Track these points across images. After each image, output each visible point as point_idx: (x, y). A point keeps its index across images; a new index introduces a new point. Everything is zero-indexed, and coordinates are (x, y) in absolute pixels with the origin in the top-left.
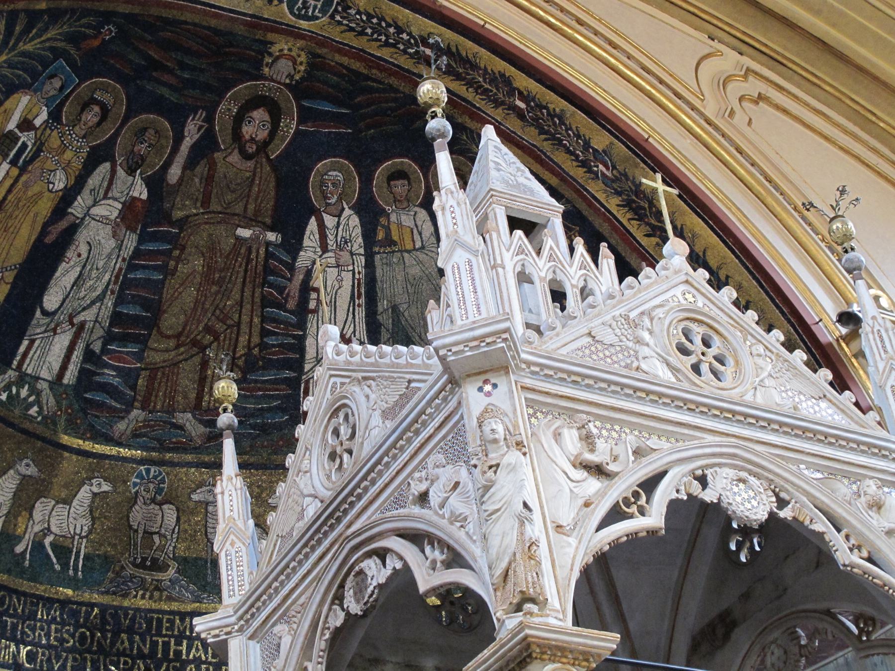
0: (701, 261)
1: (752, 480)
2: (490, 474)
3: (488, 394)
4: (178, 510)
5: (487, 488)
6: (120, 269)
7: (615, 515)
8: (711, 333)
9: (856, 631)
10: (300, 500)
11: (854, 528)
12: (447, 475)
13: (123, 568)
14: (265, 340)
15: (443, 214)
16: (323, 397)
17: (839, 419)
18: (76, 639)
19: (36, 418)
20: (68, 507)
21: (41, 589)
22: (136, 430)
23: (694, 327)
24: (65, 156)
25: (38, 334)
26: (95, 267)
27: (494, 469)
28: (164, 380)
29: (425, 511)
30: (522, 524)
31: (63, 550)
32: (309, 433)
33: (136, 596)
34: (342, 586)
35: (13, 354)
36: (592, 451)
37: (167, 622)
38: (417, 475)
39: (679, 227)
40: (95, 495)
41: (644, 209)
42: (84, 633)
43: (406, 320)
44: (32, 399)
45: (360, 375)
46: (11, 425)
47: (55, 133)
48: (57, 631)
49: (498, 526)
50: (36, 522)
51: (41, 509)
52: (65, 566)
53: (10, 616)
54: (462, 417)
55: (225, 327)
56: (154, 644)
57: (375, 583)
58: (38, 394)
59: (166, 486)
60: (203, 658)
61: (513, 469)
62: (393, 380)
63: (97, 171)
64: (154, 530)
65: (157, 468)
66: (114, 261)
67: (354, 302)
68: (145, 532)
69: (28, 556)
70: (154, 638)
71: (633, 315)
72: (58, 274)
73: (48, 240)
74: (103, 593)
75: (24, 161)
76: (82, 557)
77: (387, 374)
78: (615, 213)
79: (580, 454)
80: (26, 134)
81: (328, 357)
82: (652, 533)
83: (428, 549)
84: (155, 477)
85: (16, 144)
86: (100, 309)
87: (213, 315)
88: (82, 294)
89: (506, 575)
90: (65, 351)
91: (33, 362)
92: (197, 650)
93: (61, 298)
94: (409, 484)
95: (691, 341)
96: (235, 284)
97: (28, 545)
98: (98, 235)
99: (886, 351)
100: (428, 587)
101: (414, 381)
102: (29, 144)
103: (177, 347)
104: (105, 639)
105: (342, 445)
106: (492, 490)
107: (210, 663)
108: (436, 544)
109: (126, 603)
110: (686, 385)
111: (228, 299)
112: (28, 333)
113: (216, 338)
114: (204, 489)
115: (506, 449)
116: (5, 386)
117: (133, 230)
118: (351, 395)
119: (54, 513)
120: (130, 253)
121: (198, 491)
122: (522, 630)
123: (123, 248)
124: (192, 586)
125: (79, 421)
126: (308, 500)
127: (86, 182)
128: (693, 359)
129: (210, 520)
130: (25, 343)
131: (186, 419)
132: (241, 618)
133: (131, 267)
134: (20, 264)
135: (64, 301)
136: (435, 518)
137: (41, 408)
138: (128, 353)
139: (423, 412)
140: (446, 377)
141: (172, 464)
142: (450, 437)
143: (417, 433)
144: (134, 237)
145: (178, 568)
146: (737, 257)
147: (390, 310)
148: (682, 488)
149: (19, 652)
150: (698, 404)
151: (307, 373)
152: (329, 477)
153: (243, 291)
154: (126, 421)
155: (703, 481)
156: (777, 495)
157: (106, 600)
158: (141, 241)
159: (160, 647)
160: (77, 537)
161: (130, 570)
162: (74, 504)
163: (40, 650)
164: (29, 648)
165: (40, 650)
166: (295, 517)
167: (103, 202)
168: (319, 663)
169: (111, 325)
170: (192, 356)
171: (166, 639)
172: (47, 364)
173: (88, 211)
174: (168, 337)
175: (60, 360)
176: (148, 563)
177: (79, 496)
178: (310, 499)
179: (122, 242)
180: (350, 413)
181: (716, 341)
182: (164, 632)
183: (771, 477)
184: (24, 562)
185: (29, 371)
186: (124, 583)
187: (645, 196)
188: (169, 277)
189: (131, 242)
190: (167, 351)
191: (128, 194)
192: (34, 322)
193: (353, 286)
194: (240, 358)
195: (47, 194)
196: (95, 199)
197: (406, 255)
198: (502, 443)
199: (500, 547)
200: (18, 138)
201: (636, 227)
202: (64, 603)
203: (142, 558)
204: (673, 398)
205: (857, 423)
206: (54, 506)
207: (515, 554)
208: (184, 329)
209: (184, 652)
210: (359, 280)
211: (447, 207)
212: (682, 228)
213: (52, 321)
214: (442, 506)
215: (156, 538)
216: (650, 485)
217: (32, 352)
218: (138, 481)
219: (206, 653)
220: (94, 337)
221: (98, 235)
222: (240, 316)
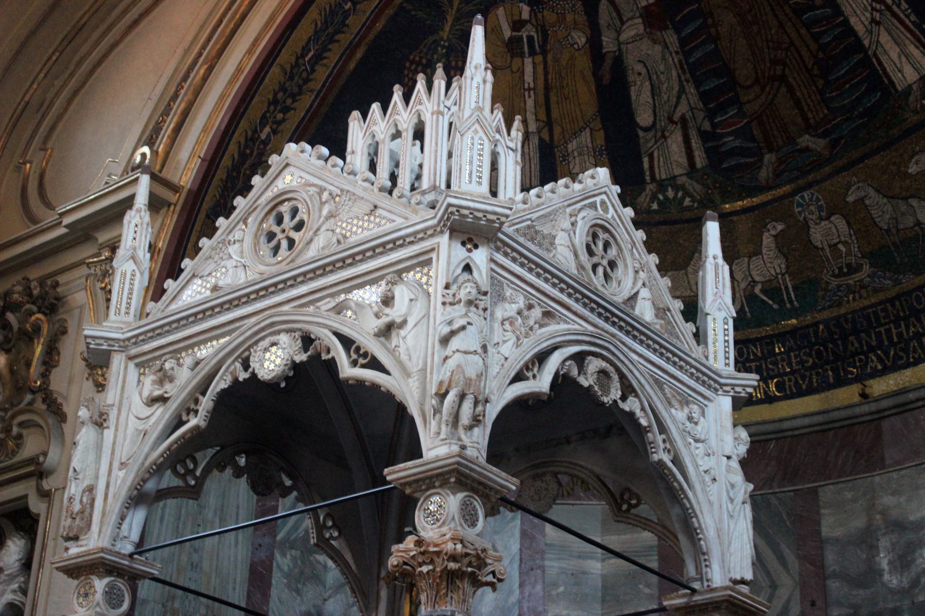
4: (842, 215)
6: (680, 61)
13: (827, 283)
14: (821, 41)
18: (814, 356)
19: (693, 206)
20: (761, 257)
21: (768, 330)
22: (775, 171)
24: (568, 20)
25: (652, 147)
26: (659, 73)
28: (771, 120)
31: (772, 290)
33: (848, 302)
35: (642, 172)
37: (882, 312)
40: (775, 236)
42: (819, 349)
44: (680, 194)
46: (675, 222)
47: (546, 13)
48: (796, 357)
50: (740, 281)
51: (738, 269)
52: (781, 302)
53: (753, 361)
56: (878, 335)
58: (683, 187)
63: (600, 11)
64: (835, 241)
65: (808, 192)
66: (670, 59)
68: (830, 246)
69: (747, 309)
70: (877, 330)
72: (634, 98)
73: (606, 80)
74: (820, 311)
75: (539, 47)
76: (791, 290)
80: (524, 30)
84: (811, 200)
85: (523, 41)
86: (688, 99)
87: (769, 48)
88: (665, 97)
90: (683, 145)
91: (662, 170)
92: (915, 326)
93: (651, 111)
96: (766, 14)
97: (742, 302)
98: (641, 50)
102: (532, 34)
103: (763, 89)
104: (837, 346)
109: (843, 311)
111: (770, 29)
112: (643, 151)
114: (853, 188)
116: (650, 199)
117: (666, 28)
119: (751, 267)
120: (678, 45)
121: (850, 193)
123: (669, 45)
124: (888, 275)
125: (729, 189)
127: (598, 24)
129: (873, 212)
130: (646, 160)
131: (806, 140)
133: (687, 54)
134: (598, 112)
135: (654, 112)
137: (691, 196)
138: (731, 117)
141: (818, 182)
144: (671, 32)
149: (768, 387)
150: (239, 298)
153: (776, 16)
154: (764, 168)
157: (826, 315)
158: (678, 31)
159: (884, 336)
160: (780, 276)
161: (834, 283)
162: (764, 251)
163: (786, 379)
164: (775, 381)
165: (786, 379)
167: (624, 27)
169: (705, 104)
170: (778, 91)
171: (887, 327)
172: (674, 163)
173: (618, 41)
175: (684, 154)
176: (845, 270)
177: (765, 243)
179: (664, 41)
182: (883, 322)
184: (746, 315)
185: (664, 177)
186: (835, 294)
188: (719, 42)
189: (671, 37)
190: (758, 97)
191: (638, 8)
192: (642, 141)
194: (812, 68)
195: (577, 54)
196: (616, 30)
200: (521, 38)
202: (793, 331)
203: (838, 268)
206: (749, 261)
208: (756, 73)
209: (904, 332)
213: (656, 132)
215: (841, 247)
217: (656, 163)
218: (800, 209)
220: (699, 120)
221: (641, 50)
222: (788, 36)
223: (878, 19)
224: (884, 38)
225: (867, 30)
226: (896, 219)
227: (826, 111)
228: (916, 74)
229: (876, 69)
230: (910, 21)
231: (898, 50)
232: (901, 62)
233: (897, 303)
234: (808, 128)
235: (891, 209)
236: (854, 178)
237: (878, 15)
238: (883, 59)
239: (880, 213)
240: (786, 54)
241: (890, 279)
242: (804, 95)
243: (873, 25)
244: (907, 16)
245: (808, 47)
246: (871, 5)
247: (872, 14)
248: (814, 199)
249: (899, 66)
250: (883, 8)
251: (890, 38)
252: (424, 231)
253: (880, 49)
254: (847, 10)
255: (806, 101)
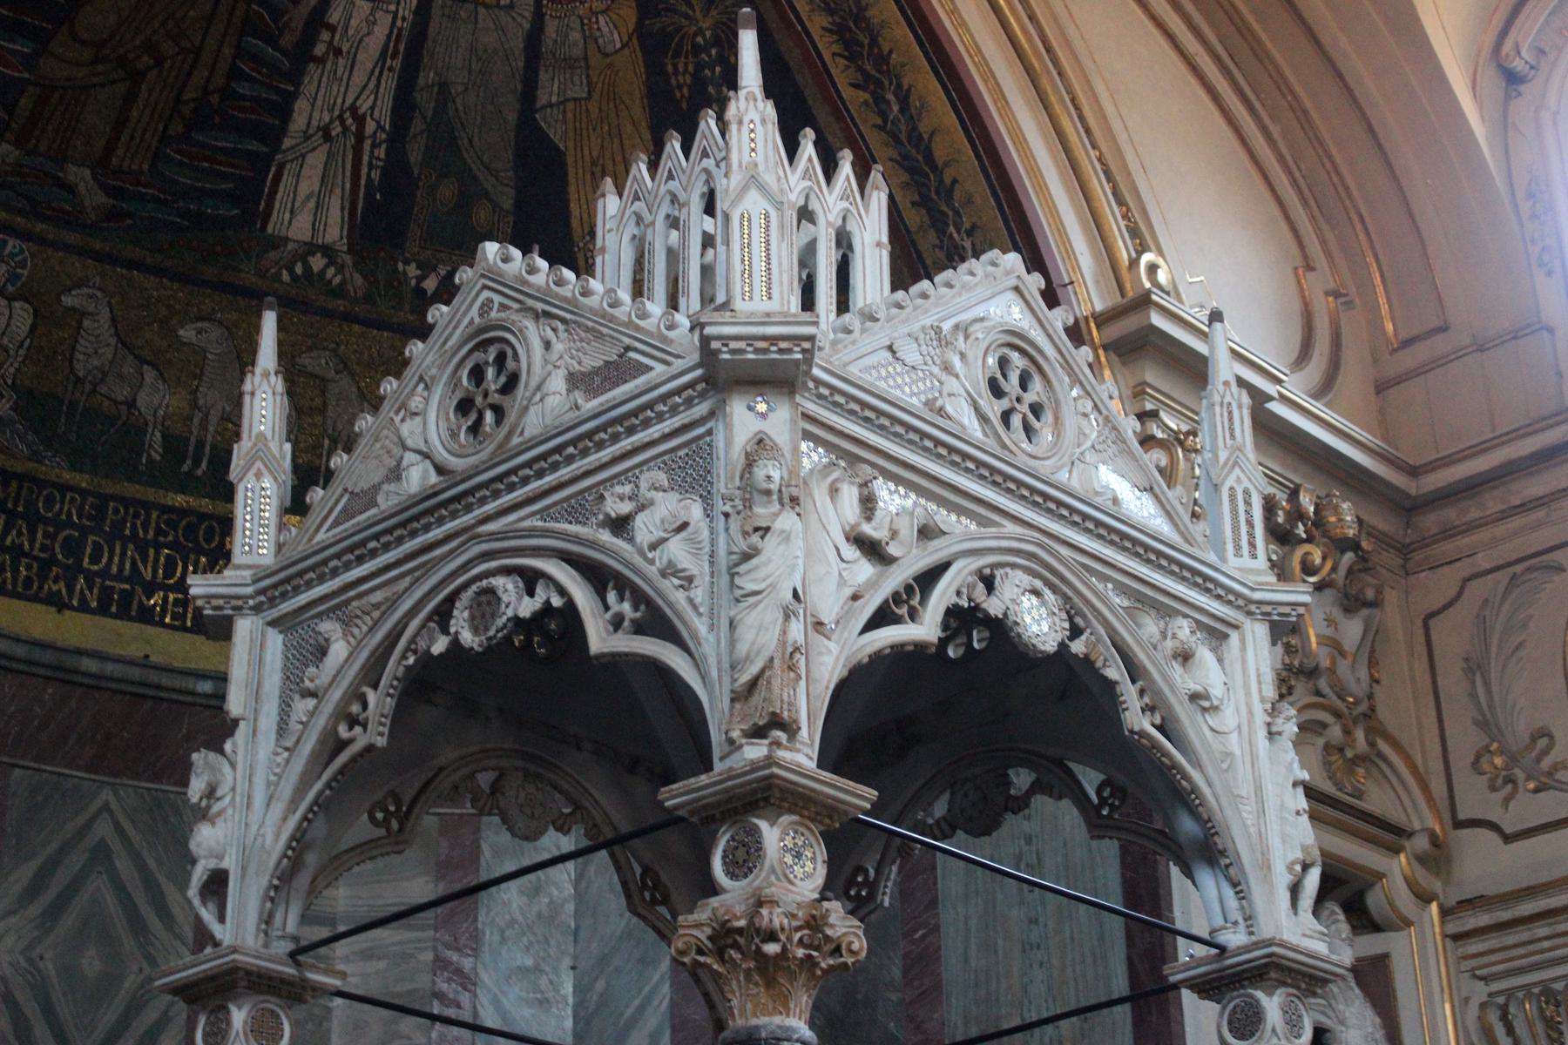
0: (922, 148)
1: (1047, 593)
2: (755, 538)
3: (763, 416)
4: (36, 313)
5: (747, 557)
7: (882, 617)
8: (1033, 370)
9: (1095, 799)
10: (397, 451)
11: (1152, 682)
12: (667, 506)
14: (234, 85)
15: (739, 130)
16: (465, 313)
17: (1161, 525)
23: (1015, 356)
27: (760, 533)
29: (620, 544)
30: (787, 617)
32: (430, 359)
34: (451, 600)
36: (869, 519)
38: (619, 489)
39: (906, 87)
41: (861, 45)
43: (457, 109)
45: (540, 306)
49: (754, 614)
54: (710, 432)
55: (177, 49)
57: (510, 613)
59: (26, 273)
60: (27, 546)
61: (786, 537)
62: (599, 336)
65: (18, 242)
67: (384, 62)
71: (947, 326)
77: (590, 324)
78: (816, 38)
79: (857, 524)
81: (486, 259)
82: (920, 647)
83: (612, 597)
84: (12, 255)
89: (753, 684)
92: (20, 534)
94: (602, 497)
95: (1005, 376)
99: (1232, 436)
100: (606, 650)
101: (636, 350)
103: (95, 61)
105: (486, 395)
106: (755, 561)
107: (36, 558)
108: (627, 594)
110: (991, 444)
113: (159, 63)
114: (85, 290)
115: (778, 507)
118: (521, 331)
121: (74, 293)
122: (769, 766)
126: (410, 457)
128: (1005, 404)
131: (79, 176)
132: (262, 592)
136: (638, 560)
138: (13, 52)
139: (649, 405)
140: (699, 372)
141: (43, 241)
142: (681, 453)
143: (631, 431)
145: (16, 403)
146: (978, 157)
147: (436, 89)
148: (965, 590)
150: (1007, 477)
151: (284, 151)
152: (454, 435)
155: (989, 584)
156: (1071, 619)
166: (382, 472)
168: (389, 695)
170: (113, 82)
174: (83, 43)
178: (418, 457)
180: (510, 352)
181: (1037, 384)
183: (1070, 593)
187: (868, 25)
193: (389, 37)
197: (482, 10)
198: (775, 497)
199: (753, 644)
201: (841, 67)
204: (980, 464)
205: (1181, 534)
207: (772, 660)
210: (400, 30)
211: (746, 120)
212: (909, 91)
214: (653, 547)
216: (928, 579)
219: (32, 541)
223: (333, 133)
224: (316, 160)
225: (305, 132)
226: (105, 374)
227: (146, 167)
228: (310, 234)
229: (264, 181)
230: (369, 175)
231: (317, 189)
232: (304, 203)
233: (14, 484)
234: (101, 164)
235: (110, 357)
236: (98, 279)
237: (339, 129)
238: (287, 180)
239: (91, 351)
240: (178, 54)
241: (29, 446)
242: (139, 121)
243: (321, 133)
244: (371, 166)
245: (212, 71)
246: (342, 111)
247: (331, 122)
248: (17, 259)
249: (297, 204)
250: (353, 128)
251: (321, 167)
252: (1238, 595)
253: (294, 166)
254: (309, 86)
255: (134, 129)
